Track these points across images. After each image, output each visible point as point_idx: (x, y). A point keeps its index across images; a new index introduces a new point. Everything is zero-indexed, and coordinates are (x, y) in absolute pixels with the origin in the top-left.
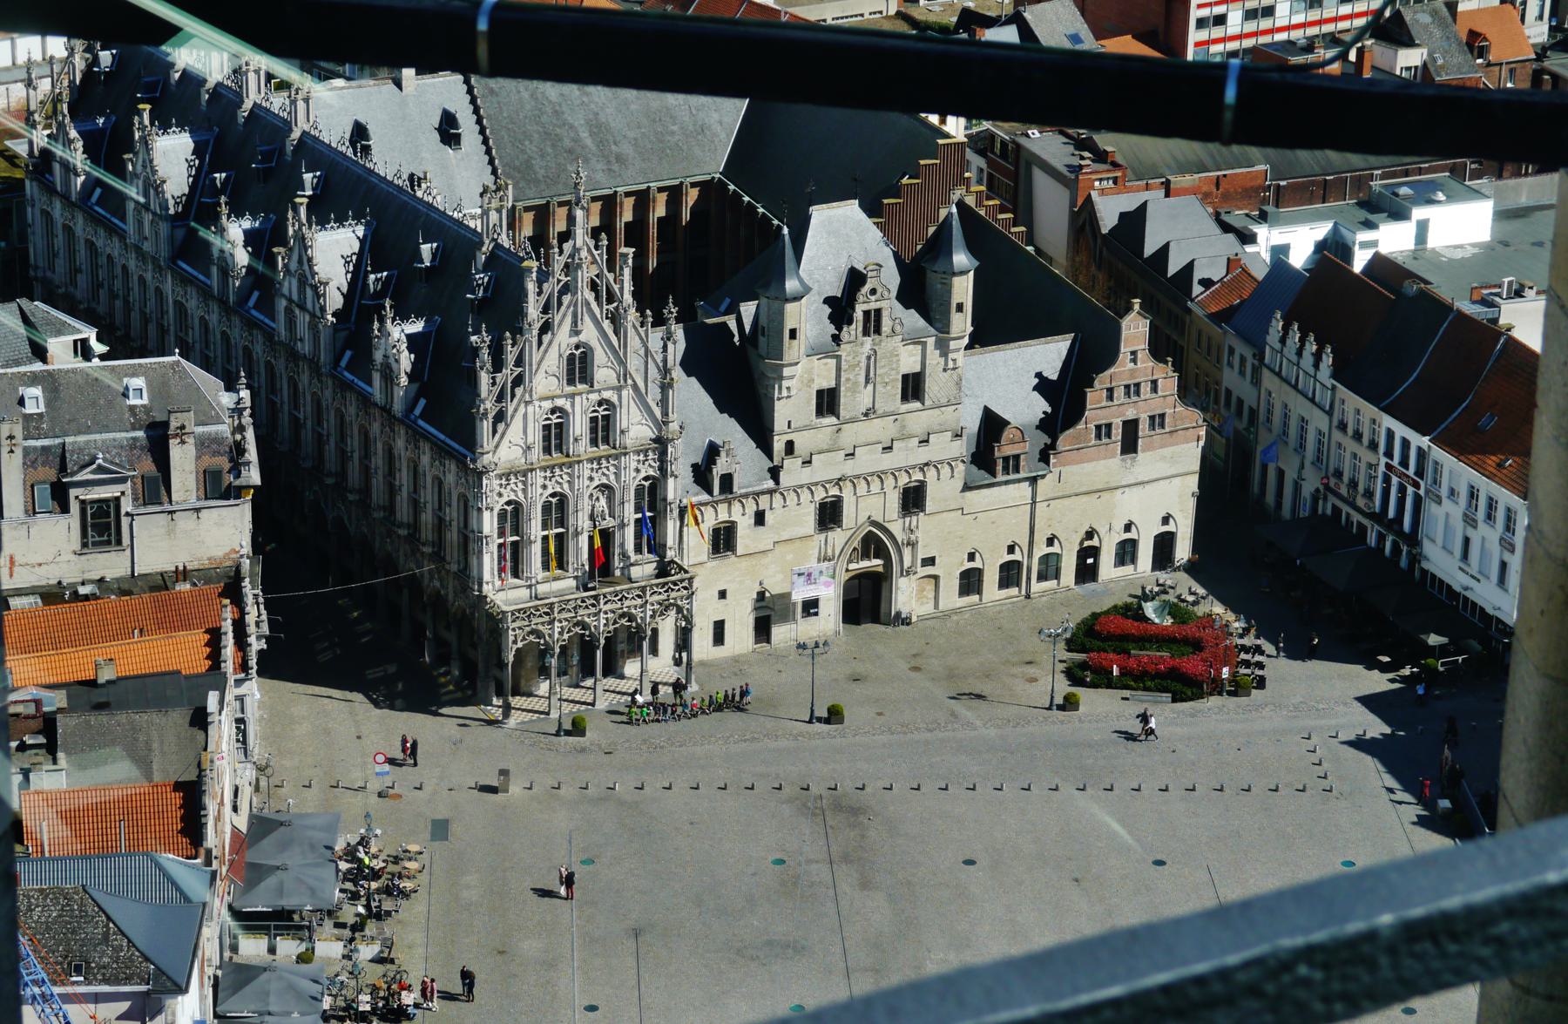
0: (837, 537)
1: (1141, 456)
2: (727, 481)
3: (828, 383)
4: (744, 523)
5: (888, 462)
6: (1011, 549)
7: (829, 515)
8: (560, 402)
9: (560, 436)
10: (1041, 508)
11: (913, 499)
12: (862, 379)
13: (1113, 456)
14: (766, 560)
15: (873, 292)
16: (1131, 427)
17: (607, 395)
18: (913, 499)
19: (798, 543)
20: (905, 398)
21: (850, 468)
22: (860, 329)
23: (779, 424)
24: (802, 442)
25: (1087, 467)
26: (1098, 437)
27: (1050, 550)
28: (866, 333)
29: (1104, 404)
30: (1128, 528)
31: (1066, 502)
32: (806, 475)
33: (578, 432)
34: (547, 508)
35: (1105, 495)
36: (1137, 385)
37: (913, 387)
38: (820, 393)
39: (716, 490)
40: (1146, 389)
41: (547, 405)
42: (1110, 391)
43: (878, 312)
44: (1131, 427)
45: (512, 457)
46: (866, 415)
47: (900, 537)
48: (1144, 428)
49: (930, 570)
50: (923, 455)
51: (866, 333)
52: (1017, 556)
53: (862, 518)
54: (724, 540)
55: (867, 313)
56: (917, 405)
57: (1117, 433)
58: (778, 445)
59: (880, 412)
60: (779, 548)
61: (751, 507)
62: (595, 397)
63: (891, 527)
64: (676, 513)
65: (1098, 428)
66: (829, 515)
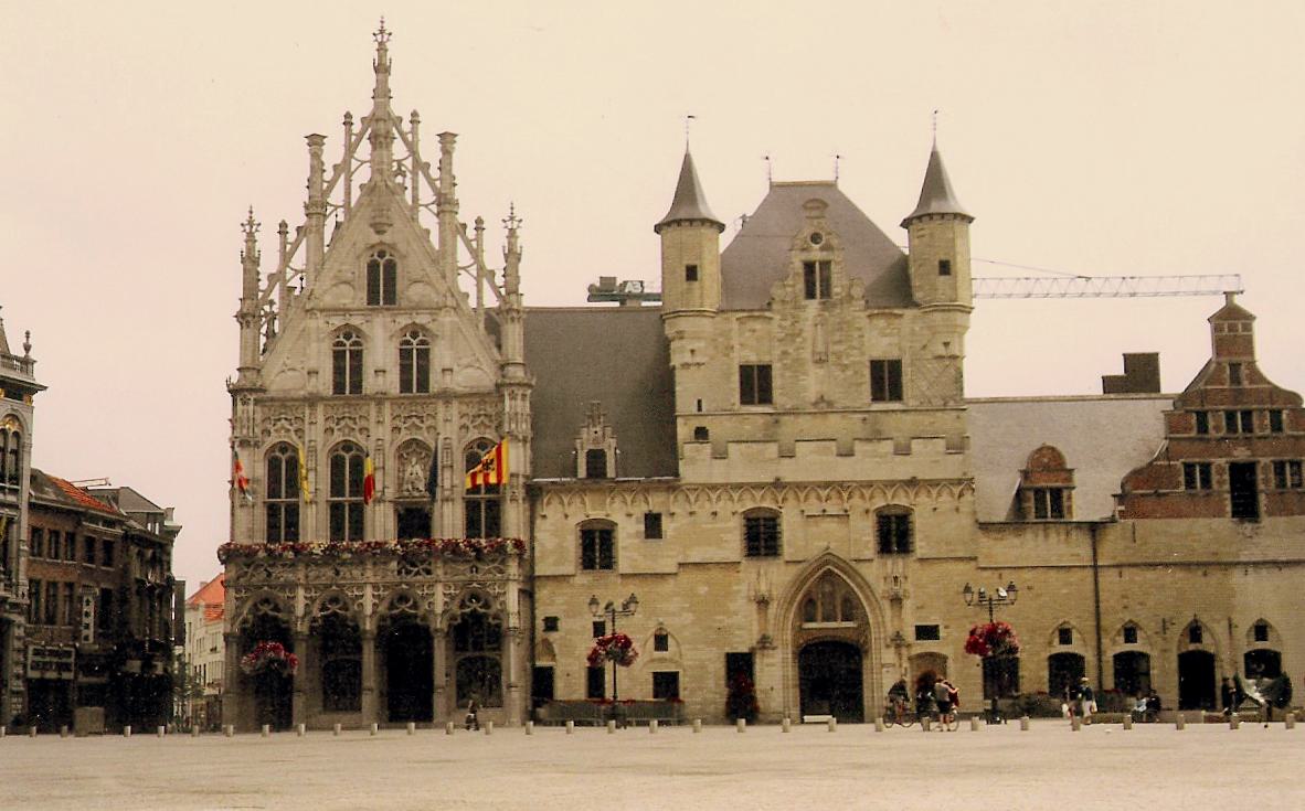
0: (775, 577)
1: (1266, 521)
2: (596, 458)
3: (753, 358)
4: (628, 532)
5: (845, 470)
6: (1065, 636)
7: (761, 537)
8: (356, 321)
9: (357, 370)
10: (1108, 579)
11: (894, 534)
12: (807, 354)
13: (1219, 514)
14: (669, 586)
15: (815, 238)
16: (1242, 475)
17: (422, 319)
18: (894, 534)
19: (715, 574)
20: (877, 395)
21: (789, 472)
22: (801, 286)
23: (684, 402)
24: (716, 428)
25: (1179, 526)
26: (1190, 483)
27: (1129, 647)
28: (810, 295)
29: (1193, 434)
30: (1261, 631)
31: (1150, 575)
32: (718, 473)
33: (380, 366)
34: (337, 464)
35: (1216, 577)
36: (1247, 414)
37: (886, 380)
38: (745, 370)
39: (582, 472)
40: (1262, 425)
41: (338, 321)
42: (1202, 417)
43: (826, 264)
44: (1242, 475)
45: (289, 385)
46: (815, 404)
47: (880, 588)
48: (1265, 481)
49: (929, 646)
50: (903, 469)
51: (810, 295)
52: (1074, 648)
53: (815, 549)
54: (597, 546)
55: (809, 267)
56: (895, 406)
57: (1222, 483)
58: (684, 431)
59: (838, 406)
60: (686, 577)
61: (641, 509)
62: (404, 321)
63: (863, 569)
64: (521, 493)
65: (1189, 468)
66: (761, 537)
